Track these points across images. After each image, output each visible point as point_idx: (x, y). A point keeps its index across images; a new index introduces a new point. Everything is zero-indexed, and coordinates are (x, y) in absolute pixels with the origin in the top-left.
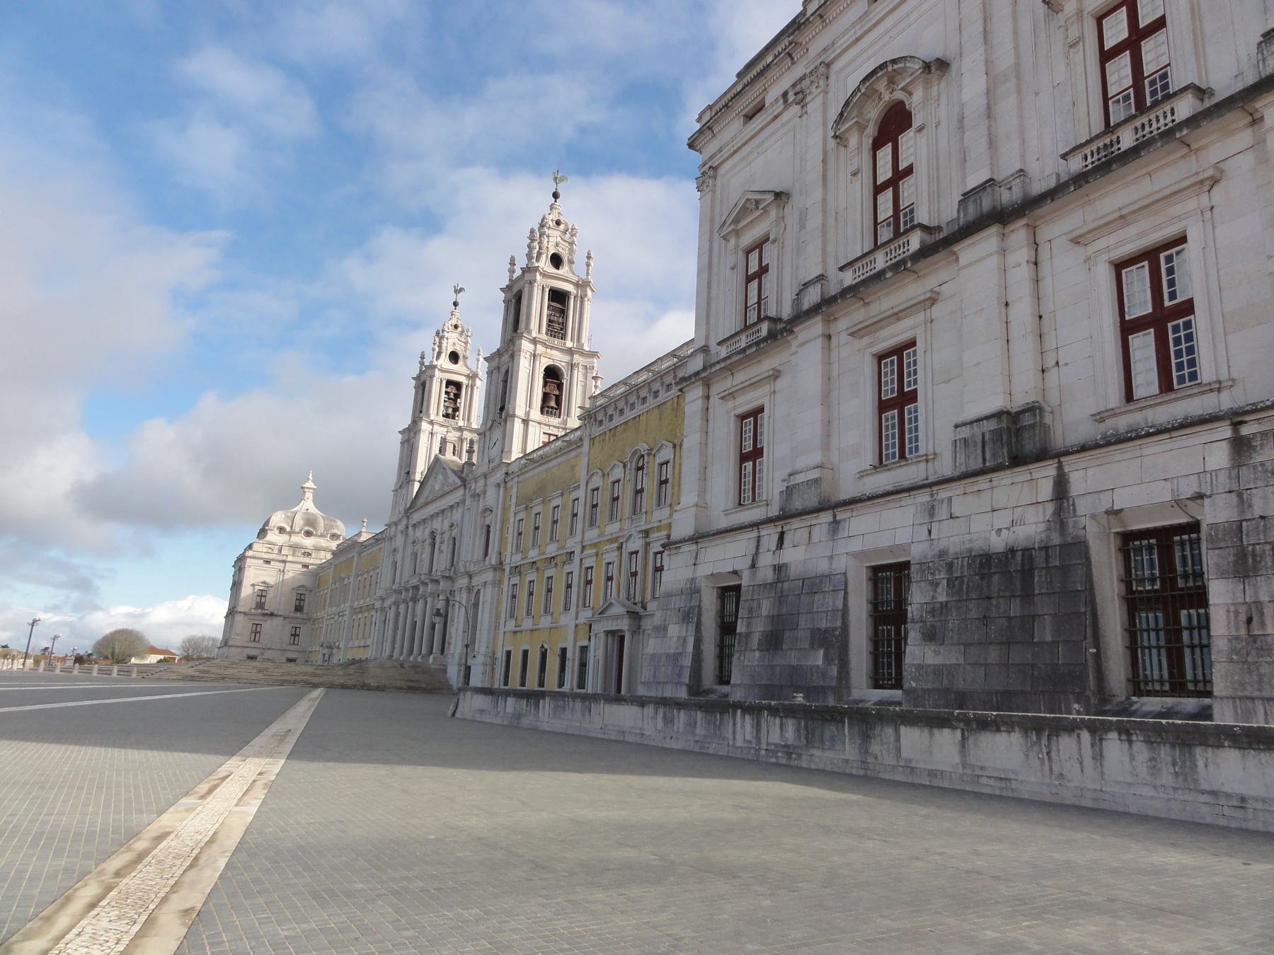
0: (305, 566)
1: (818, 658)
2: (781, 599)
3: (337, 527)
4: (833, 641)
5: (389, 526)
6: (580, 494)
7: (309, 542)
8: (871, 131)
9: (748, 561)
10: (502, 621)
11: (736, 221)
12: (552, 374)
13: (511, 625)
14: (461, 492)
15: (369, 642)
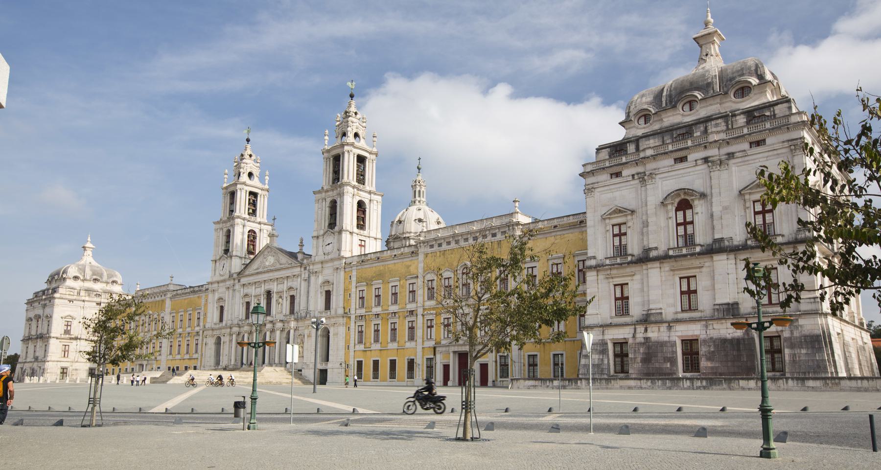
0: (99, 304)
1: (668, 365)
2: (649, 348)
3: (116, 276)
4: (673, 361)
5: (209, 283)
6: (420, 280)
7: (98, 286)
9: (631, 335)
10: (352, 345)
11: (610, 214)
12: (361, 205)
13: (361, 347)
14: (299, 269)
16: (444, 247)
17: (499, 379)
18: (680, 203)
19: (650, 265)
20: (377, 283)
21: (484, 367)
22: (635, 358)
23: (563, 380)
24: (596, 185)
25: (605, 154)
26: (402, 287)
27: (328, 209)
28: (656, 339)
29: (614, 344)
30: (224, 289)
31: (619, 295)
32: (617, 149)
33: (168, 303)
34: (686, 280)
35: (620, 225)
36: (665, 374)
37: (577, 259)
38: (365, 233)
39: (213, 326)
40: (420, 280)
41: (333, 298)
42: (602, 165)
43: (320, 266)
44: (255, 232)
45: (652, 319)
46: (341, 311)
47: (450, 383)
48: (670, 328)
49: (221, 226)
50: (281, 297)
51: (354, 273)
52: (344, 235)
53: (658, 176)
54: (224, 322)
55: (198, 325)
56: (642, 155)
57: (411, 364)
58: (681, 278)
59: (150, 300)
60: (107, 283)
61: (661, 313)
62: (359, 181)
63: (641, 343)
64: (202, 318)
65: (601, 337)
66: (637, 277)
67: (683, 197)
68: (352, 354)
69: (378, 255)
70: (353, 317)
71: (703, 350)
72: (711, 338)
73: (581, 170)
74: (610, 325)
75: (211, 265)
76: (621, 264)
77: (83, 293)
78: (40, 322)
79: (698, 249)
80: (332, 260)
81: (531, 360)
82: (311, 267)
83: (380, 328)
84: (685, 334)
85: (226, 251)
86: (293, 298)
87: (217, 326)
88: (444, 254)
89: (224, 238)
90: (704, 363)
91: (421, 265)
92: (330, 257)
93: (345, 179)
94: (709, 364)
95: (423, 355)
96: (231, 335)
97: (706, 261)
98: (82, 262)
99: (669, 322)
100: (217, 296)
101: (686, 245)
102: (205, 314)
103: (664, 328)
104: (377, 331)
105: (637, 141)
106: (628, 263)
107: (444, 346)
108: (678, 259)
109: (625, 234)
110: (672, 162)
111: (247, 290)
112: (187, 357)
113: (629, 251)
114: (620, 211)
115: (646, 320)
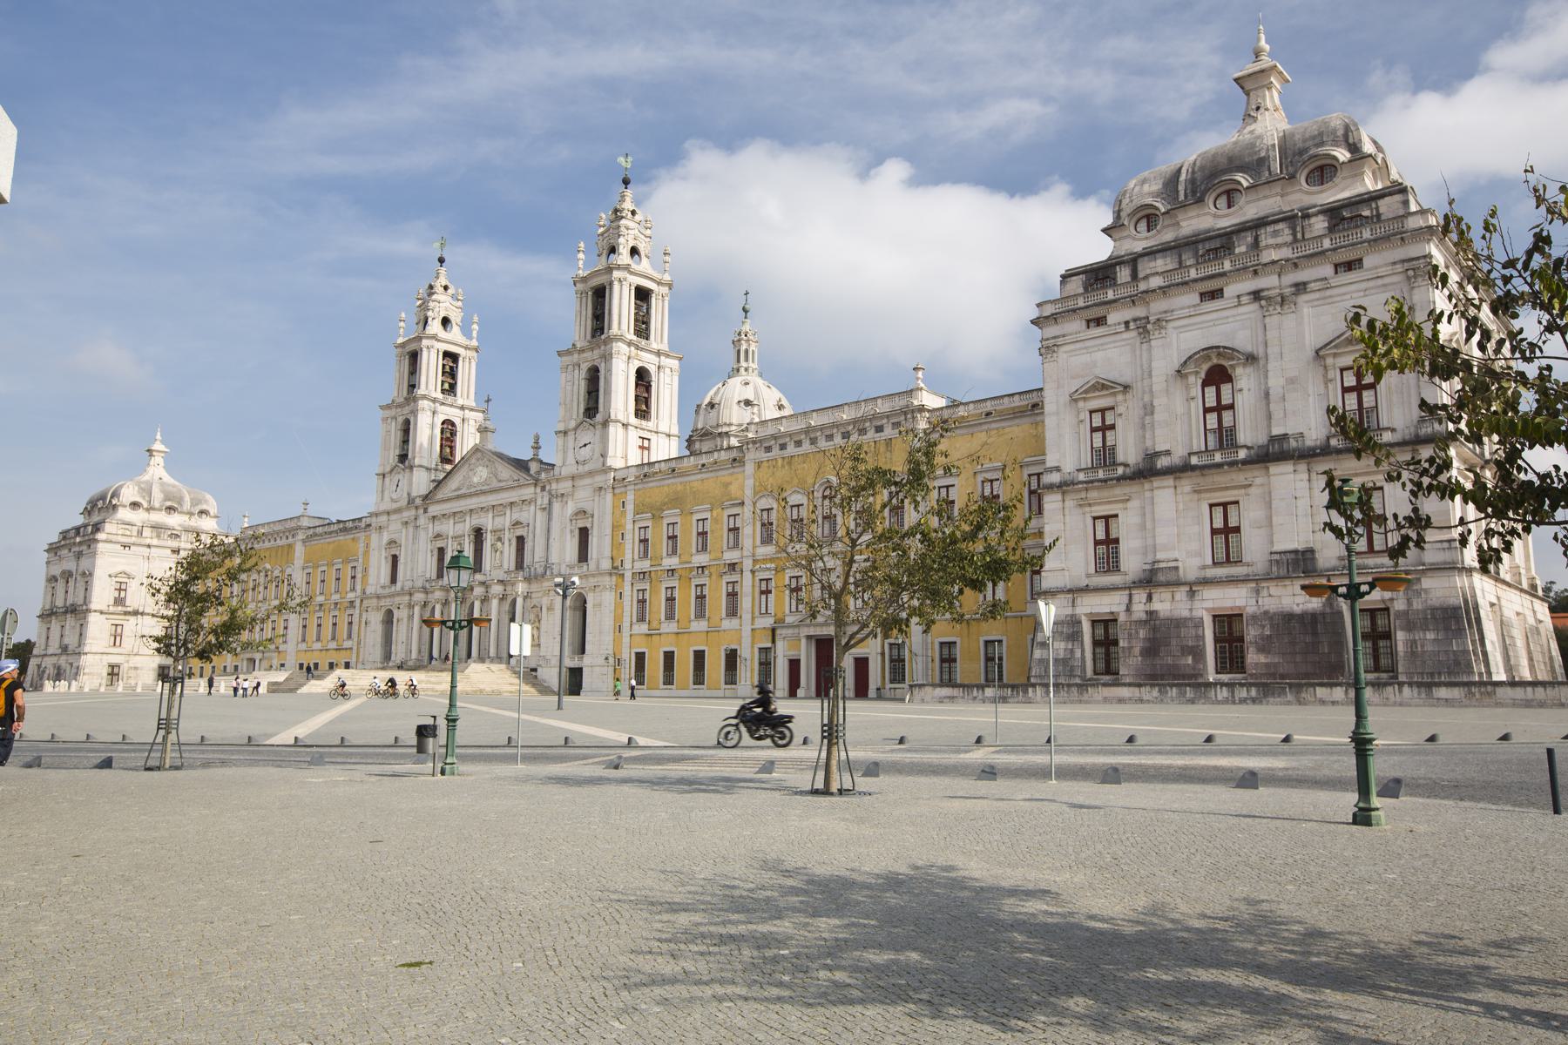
1: (1190, 660)
2: (1154, 629)
4: (1198, 653)
5: (371, 515)
6: (747, 511)
7: (174, 520)
8: (1203, 375)
10: (626, 625)
11: (1086, 392)
12: (642, 376)
14: (532, 489)
15: (347, 644)
16: (791, 449)
17: (889, 685)
18: (1210, 373)
19: (1157, 482)
20: (671, 515)
21: (862, 664)
22: (1130, 648)
23: (1003, 686)
24: (1060, 341)
25: (1076, 285)
26: (716, 521)
27: (583, 384)
28: (1167, 614)
29: (1094, 622)
30: (399, 526)
31: (1101, 535)
32: (1098, 275)
33: (299, 549)
34: (1221, 509)
35: (1103, 411)
36: (1184, 677)
37: (1026, 471)
38: (650, 425)
39: (380, 591)
40: (747, 511)
41: (593, 541)
42: (1071, 305)
43: (569, 484)
44: (453, 424)
45: (1161, 577)
46: (606, 565)
47: (800, 692)
48: (1192, 594)
49: (392, 412)
50: (499, 539)
51: (630, 497)
52: (612, 428)
53: (1171, 325)
54: (399, 584)
55: (353, 589)
56: (1142, 286)
57: (732, 658)
58: (1211, 506)
59: (267, 544)
60: (191, 514)
61: (1177, 568)
62: (638, 333)
63: (1140, 622)
64: (359, 576)
65: (1069, 611)
66: (1134, 504)
67: (1215, 361)
68: (626, 640)
69: (673, 464)
70: (628, 575)
71: (1251, 633)
72: (1266, 613)
73: (1035, 313)
74: (1086, 590)
75: (375, 482)
76: (1105, 481)
77: (147, 532)
78: (71, 583)
79: (1242, 454)
80: (591, 473)
81: (946, 651)
82: (554, 486)
83: (676, 594)
84: (1218, 604)
85: (403, 457)
86: (521, 541)
87: (387, 591)
88: (790, 463)
89: (399, 434)
90: (1253, 657)
91: (750, 483)
92: (587, 468)
93: (615, 330)
94: (1262, 659)
95: (753, 643)
96: (411, 606)
97: (1256, 476)
98: (146, 478)
99: (1191, 584)
100: (386, 538)
101: (1221, 447)
102: (365, 570)
103: (1181, 594)
104: (671, 600)
105: (1133, 261)
106: (1118, 479)
107: (790, 626)
108: (1206, 471)
109: (1112, 427)
110: (1195, 298)
111: (440, 527)
112: (333, 645)
113: (1120, 458)
114: (1104, 387)
115: (1150, 580)
